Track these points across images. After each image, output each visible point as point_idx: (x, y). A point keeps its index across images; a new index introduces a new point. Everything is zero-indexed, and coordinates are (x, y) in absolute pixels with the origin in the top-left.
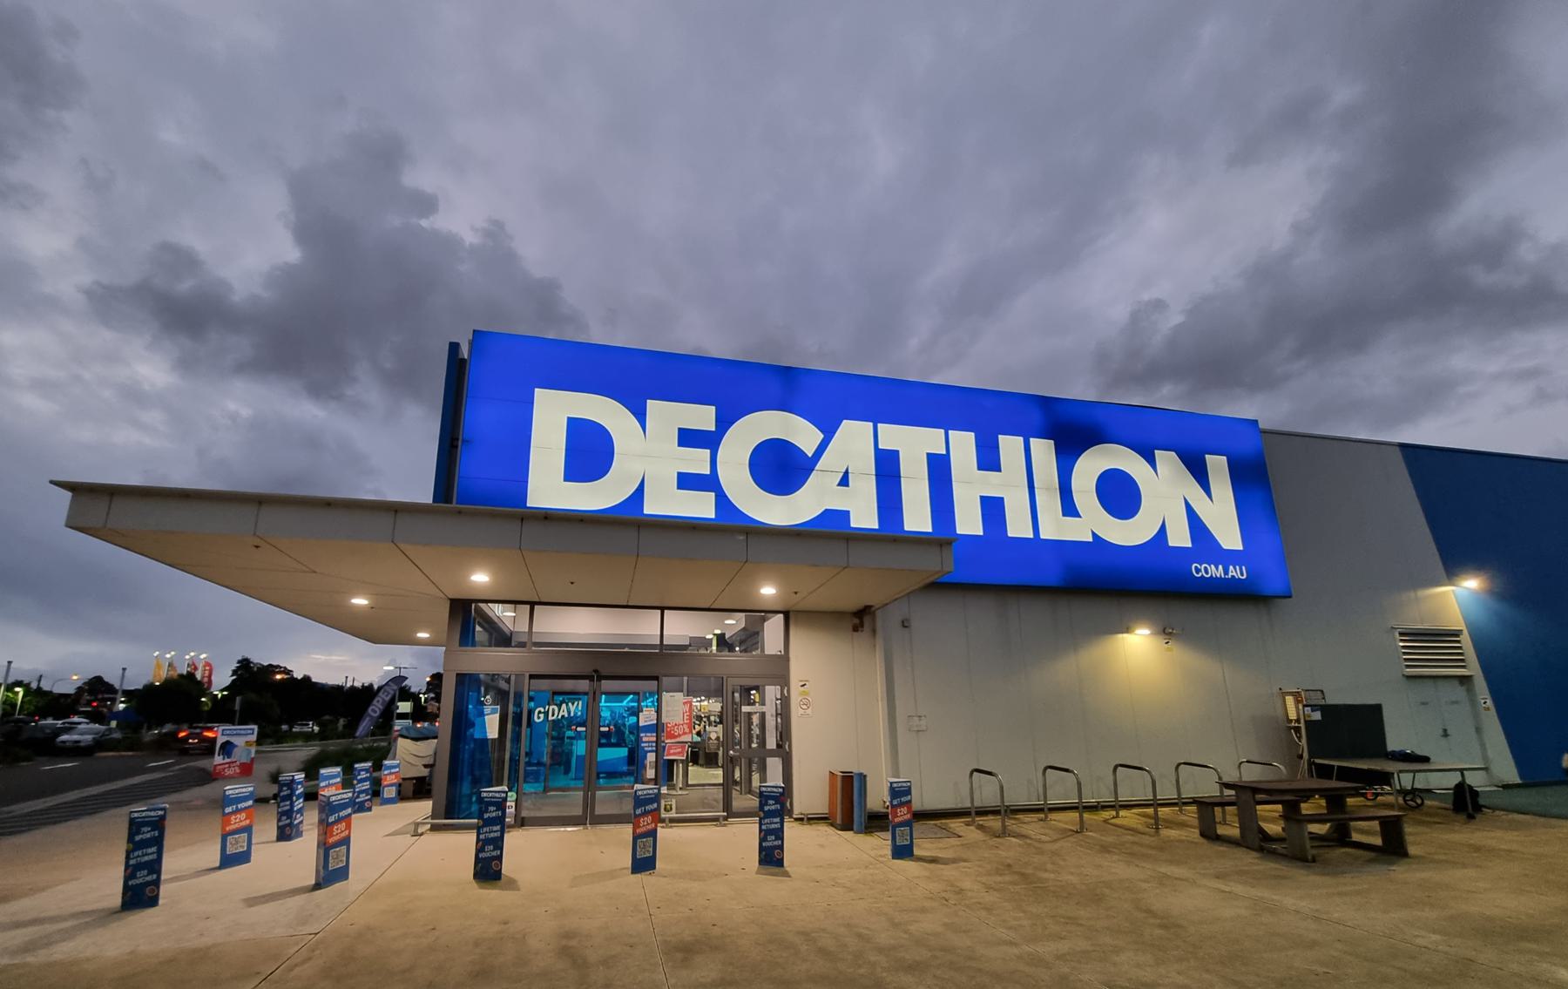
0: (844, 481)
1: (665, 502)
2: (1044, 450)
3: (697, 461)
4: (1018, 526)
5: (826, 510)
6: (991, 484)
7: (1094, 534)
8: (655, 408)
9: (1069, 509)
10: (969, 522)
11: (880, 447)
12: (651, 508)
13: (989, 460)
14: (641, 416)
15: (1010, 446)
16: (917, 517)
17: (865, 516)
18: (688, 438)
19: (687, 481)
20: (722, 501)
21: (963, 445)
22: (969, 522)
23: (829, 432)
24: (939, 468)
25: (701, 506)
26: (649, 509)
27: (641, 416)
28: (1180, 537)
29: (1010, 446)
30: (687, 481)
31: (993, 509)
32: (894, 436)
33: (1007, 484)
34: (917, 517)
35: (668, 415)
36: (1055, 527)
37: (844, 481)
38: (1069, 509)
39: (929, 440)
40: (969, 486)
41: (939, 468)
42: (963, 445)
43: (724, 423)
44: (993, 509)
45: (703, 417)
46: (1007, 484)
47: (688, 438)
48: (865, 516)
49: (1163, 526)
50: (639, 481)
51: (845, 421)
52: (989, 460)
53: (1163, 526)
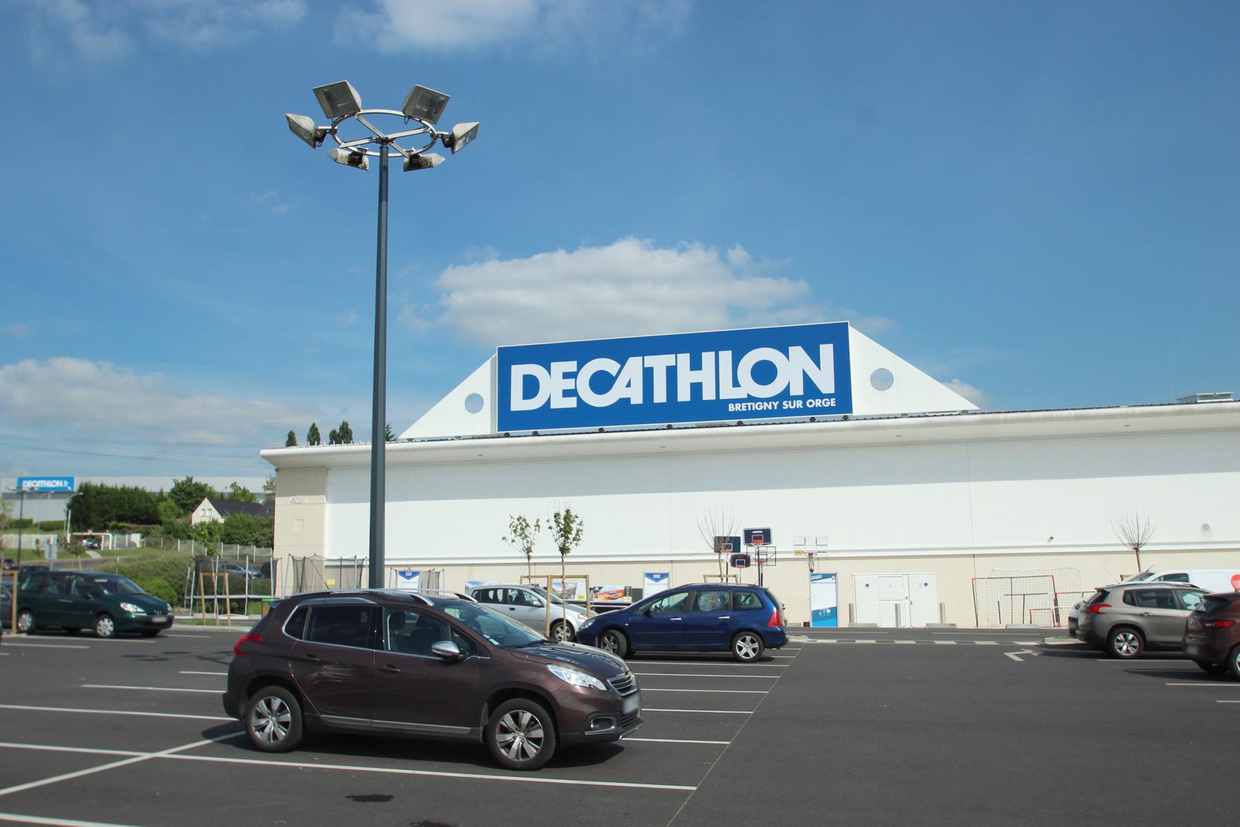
0: (629, 385)
1: (559, 403)
2: (726, 356)
3: (569, 384)
4: (708, 394)
5: (620, 399)
6: (696, 376)
7: (748, 395)
8: (554, 366)
9: (736, 383)
10: (684, 395)
11: (645, 366)
12: (553, 406)
13: (696, 365)
14: (549, 370)
15: (708, 358)
16: (660, 396)
17: (637, 398)
18: (567, 375)
19: (567, 393)
20: (580, 401)
21: (684, 359)
22: (684, 395)
23: (623, 363)
24: (672, 372)
25: (571, 403)
26: (552, 407)
27: (549, 370)
28: (797, 389)
29: (708, 358)
30: (567, 393)
31: (696, 388)
32: (651, 361)
33: (705, 376)
34: (660, 396)
35: (559, 367)
36: (727, 392)
37: (629, 385)
38: (736, 383)
39: (668, 360)
40: (686, 378)
41: (672, 372)
42: (684, 359)
43: (579, 367)
44: (696, 388)
45: (571, 366)
46: (705, 376)
47: (567, 375)
48: (637, 398)
49: (789, 385)
50: (547, 399)
51: (630, 358)
52: (696, 365)
53: (789, 385)
